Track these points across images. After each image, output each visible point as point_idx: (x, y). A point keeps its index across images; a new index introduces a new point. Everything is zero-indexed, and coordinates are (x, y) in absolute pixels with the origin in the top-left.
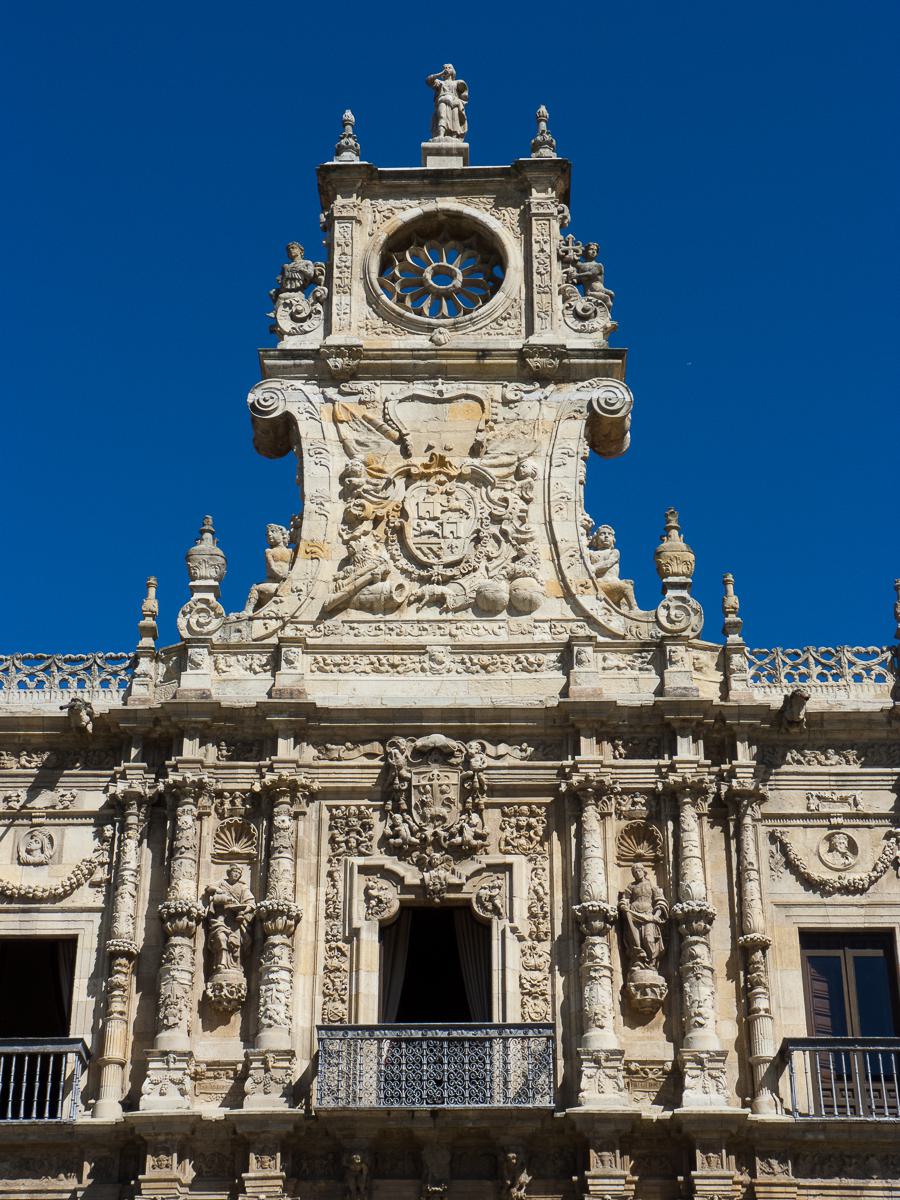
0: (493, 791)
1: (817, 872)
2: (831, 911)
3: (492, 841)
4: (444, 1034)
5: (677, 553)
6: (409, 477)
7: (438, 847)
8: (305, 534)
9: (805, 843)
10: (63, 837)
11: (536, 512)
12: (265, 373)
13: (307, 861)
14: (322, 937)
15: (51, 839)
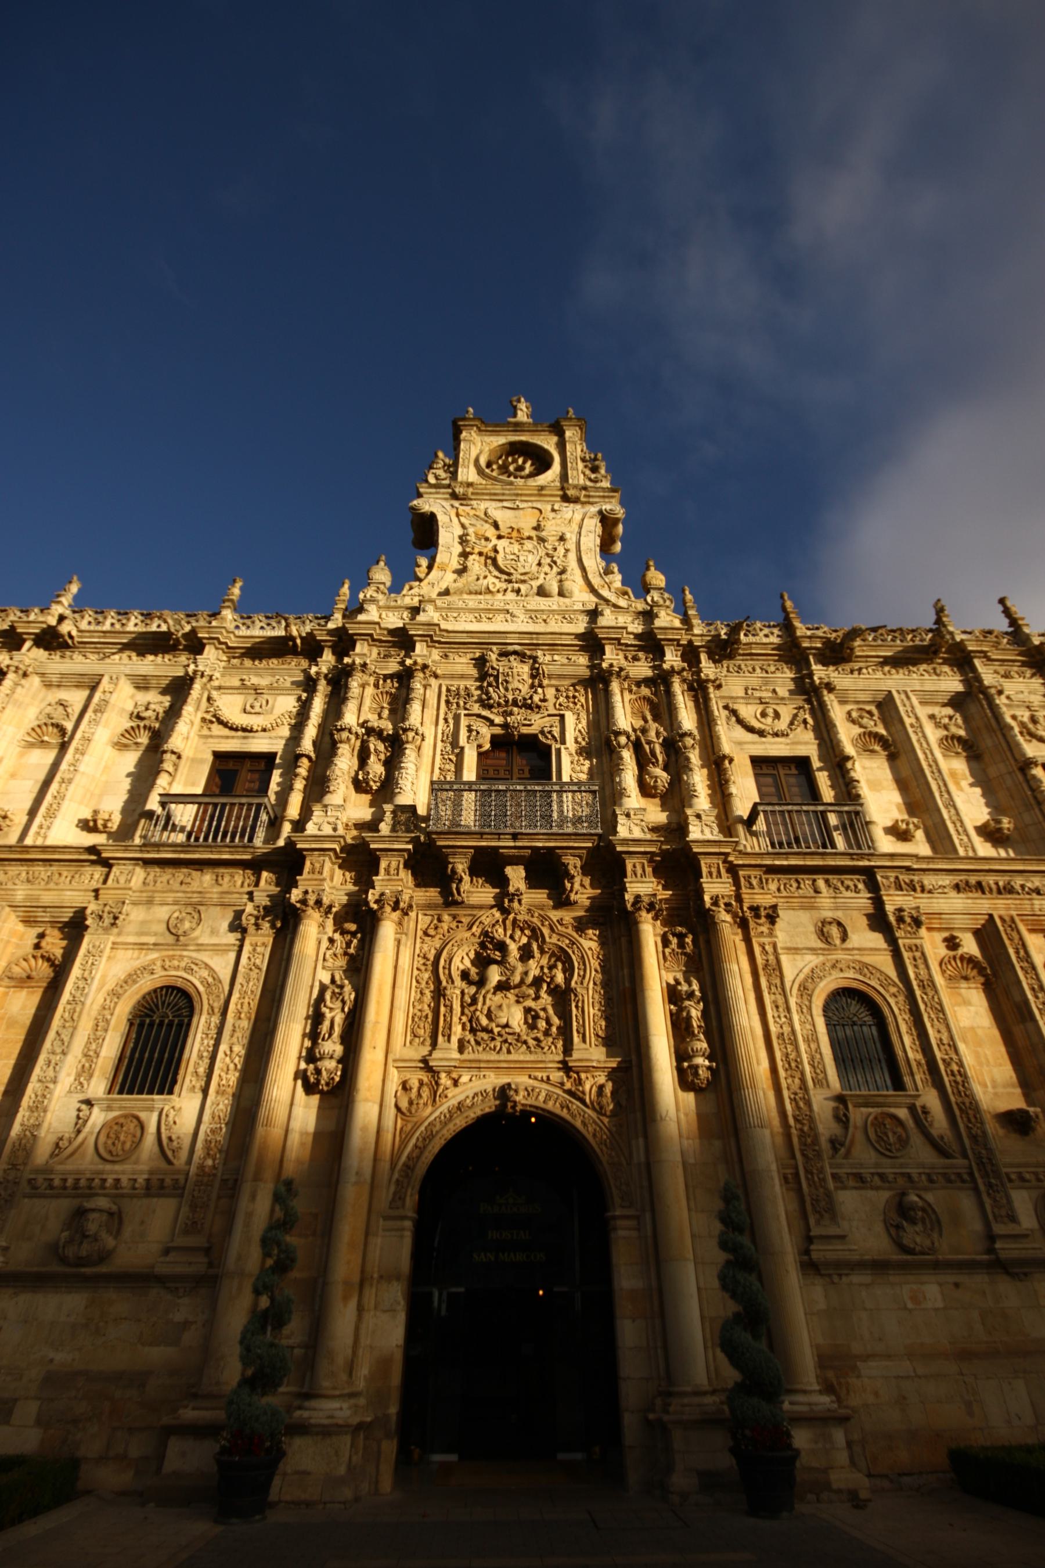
0: (550, 677)
1: (757, 725)
2: (768, 746)
3: (550, 704)
4: (521, 788)
5: (657, 578)
6: (499, 537)
7: (515, 703)
8: (438, 559)
9: (748, 712)
10: (275, 700)
11: (572, 556)
12: (420, 495)
13: (430, 713)
14: (438, 752)
15: (267, 702)
